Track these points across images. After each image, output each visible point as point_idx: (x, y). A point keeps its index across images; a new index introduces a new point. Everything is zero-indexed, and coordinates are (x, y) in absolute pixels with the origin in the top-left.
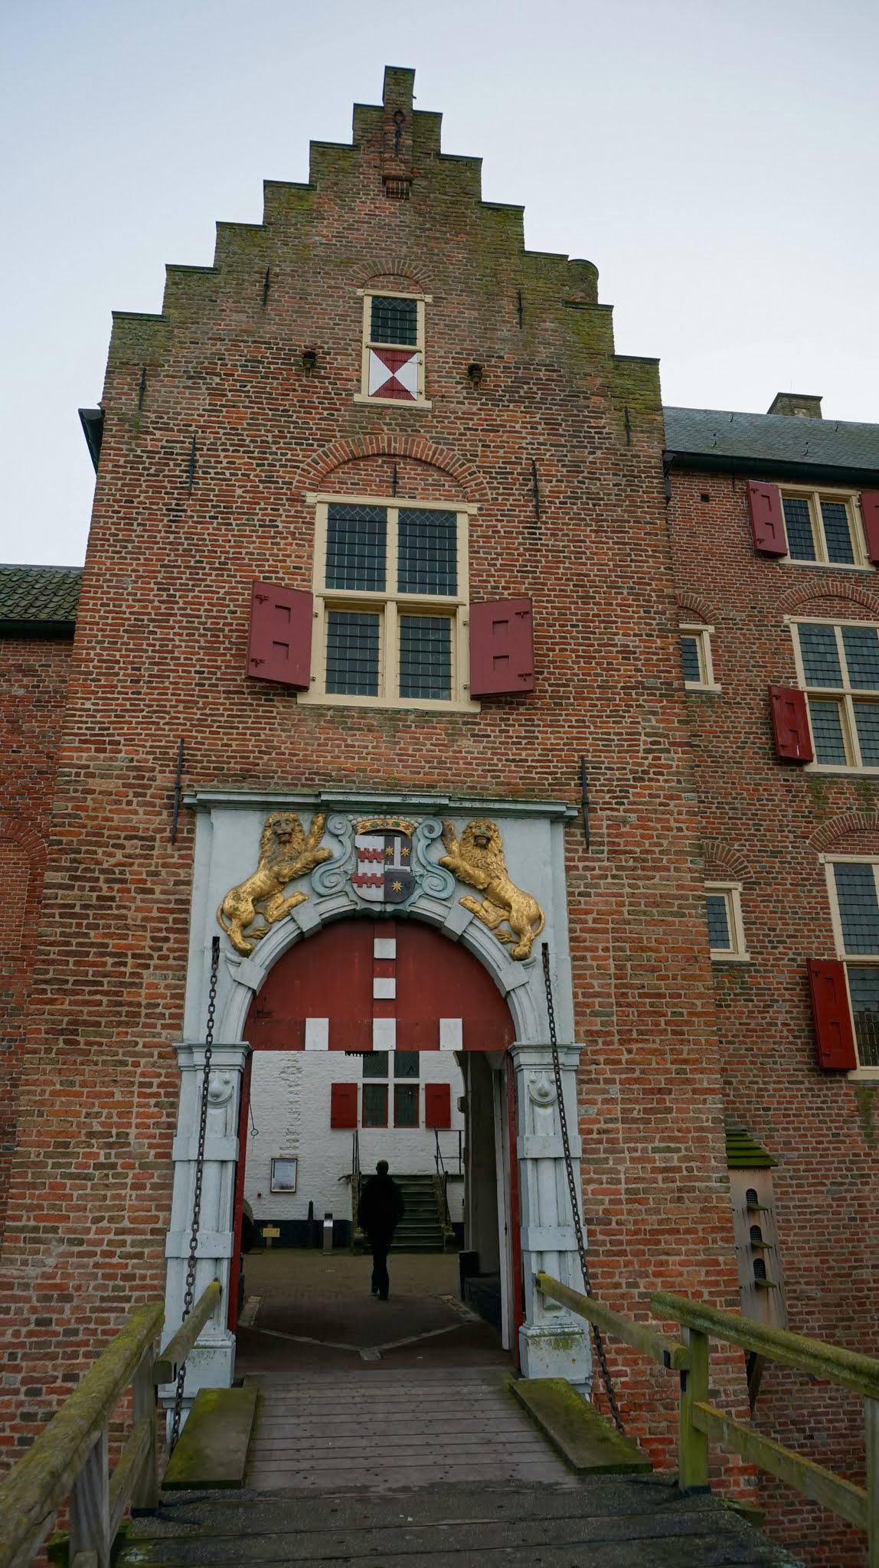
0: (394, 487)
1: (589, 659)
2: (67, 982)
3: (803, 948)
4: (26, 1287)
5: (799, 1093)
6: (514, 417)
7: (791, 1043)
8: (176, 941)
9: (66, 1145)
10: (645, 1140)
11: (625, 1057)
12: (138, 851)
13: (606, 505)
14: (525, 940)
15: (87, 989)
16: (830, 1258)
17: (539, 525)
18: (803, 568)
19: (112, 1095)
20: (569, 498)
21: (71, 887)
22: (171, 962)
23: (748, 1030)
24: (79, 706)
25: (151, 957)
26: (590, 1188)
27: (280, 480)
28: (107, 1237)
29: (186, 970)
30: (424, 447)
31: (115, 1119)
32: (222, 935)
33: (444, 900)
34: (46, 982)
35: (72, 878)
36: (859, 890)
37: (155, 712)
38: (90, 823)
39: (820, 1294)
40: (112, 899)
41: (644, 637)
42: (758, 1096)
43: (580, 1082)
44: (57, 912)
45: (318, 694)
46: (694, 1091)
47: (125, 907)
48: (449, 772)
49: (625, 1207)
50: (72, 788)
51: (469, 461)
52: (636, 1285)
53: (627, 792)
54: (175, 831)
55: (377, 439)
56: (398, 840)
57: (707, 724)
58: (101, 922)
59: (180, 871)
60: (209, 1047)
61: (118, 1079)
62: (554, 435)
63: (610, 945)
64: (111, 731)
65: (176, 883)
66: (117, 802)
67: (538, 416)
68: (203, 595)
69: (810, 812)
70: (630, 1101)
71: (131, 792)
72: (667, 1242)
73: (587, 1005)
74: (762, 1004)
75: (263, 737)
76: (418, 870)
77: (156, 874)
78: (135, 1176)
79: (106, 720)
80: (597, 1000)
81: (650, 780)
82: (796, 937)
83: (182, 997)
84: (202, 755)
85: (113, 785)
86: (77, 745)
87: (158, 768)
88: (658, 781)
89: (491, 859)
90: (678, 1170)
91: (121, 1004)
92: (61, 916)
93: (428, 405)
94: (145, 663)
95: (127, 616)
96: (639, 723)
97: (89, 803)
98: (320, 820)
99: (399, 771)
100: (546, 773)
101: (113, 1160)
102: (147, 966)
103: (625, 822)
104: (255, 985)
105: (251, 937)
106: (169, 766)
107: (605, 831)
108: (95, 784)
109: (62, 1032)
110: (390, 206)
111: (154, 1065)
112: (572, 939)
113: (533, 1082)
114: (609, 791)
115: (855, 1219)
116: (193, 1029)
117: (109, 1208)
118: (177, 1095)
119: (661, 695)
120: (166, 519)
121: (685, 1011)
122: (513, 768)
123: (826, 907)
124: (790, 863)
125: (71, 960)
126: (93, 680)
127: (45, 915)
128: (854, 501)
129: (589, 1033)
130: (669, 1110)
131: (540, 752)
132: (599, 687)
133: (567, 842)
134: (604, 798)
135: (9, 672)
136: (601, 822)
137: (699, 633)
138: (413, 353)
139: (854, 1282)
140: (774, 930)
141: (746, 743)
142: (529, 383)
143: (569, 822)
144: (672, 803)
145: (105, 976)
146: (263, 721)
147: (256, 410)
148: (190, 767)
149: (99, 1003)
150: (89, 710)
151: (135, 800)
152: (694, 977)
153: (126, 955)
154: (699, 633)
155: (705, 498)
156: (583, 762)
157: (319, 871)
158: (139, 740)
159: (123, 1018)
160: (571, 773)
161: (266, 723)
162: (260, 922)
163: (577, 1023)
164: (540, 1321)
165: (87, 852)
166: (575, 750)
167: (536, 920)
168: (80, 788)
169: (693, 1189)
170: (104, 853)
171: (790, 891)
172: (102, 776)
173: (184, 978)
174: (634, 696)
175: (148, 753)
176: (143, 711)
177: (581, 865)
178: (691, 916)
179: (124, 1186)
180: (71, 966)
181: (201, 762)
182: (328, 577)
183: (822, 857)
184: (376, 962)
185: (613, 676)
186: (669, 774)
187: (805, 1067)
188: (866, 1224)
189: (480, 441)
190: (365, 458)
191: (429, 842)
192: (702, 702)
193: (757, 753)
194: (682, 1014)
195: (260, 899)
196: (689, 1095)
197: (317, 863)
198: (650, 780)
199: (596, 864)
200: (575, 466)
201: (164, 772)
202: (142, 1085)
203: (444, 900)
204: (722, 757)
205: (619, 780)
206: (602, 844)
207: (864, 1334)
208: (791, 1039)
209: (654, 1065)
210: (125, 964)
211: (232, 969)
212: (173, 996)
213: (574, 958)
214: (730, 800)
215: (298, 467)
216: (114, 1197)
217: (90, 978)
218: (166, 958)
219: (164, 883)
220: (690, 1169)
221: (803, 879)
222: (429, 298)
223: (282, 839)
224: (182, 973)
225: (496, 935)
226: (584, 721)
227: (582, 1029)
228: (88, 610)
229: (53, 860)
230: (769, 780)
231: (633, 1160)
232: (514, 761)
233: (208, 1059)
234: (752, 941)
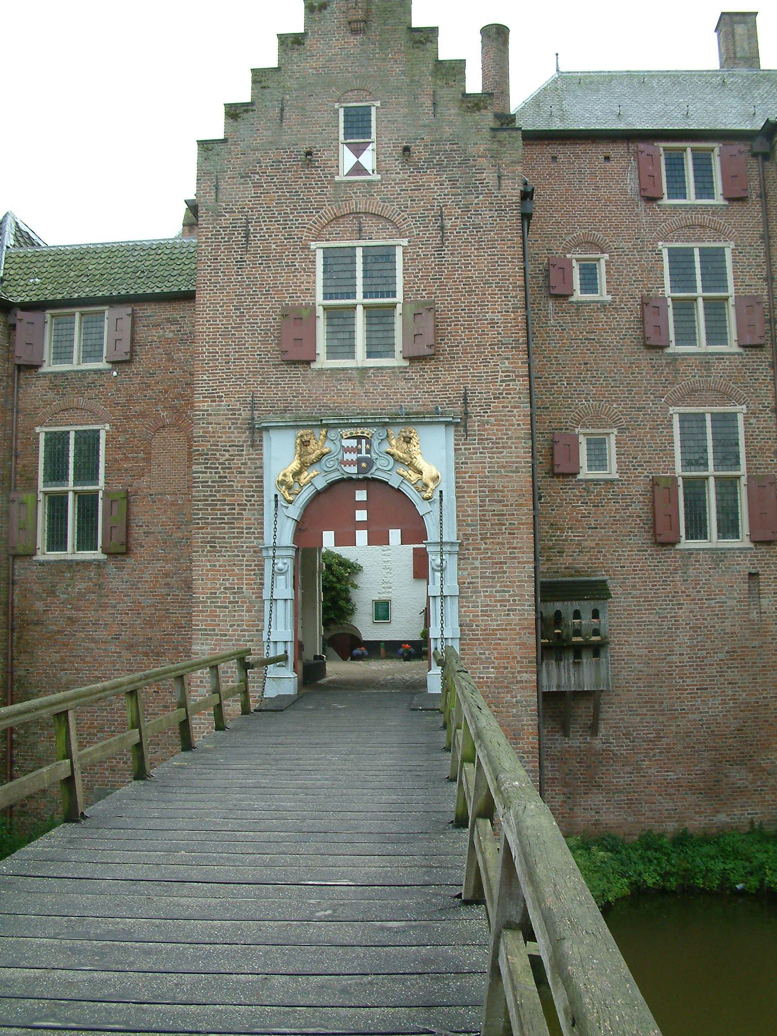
0: (360, 233)
3: (654, 469)
5: (644, 557)
6: (430, 178)
7: (642, 528)
9: (215, 593)
10: (492, 587)
13: (484, 231)
14: (429, 490)
16: (654, 650)
17: (444, 248)
18: (675, 206)
19: (234, 570)
20: (462, 229)
23: (614, 520)
25: (246, 505)
26: (463, 610)
27: (295, 237)
31: (236, 581)
32: (278, 493)
34: (199, 519)
35: (206, 468)
36: (695, 431)
38: (212, 440)
39: (646, 669)
40: (226, 477)
41: (504, 313)
42: (617, 559)
43: (460, 559)
44: (200, 485)
45: (323, 362)
46: (519, 563)
49: (480, 618)
51: (403, 211)
52: (484, 654)
54: (253, 441)
55: (349, 204)
56: (364, 441)
57: (600, 324)
60: (275, 548)
62: (454, 188)
63: (478, 489)
67: (445, 176)
68: (258, 310)
69: (666, 380)
70: (485, 568)
73: (464, 521)
74: (625, 504)
75: (294, 388)
76: (374, 456)
77: (245, 464)
80: (469, 519)
81: (503, 398)
82: (650, 462)
83: (262, 523)
85: (220, 419)
88: (508, 398)
90: (509, 601)
91: (234, 528)
93: (379, 177)
94: (231, 352)
95: (220, 326)
96: (498, 365)
97: (210, 429)
98: (324, 432)
101: (237, 599)
102: (245, 510)
103: (488, 423)
107: (476, 428)
109: (208, 542)
111: (251, 556)
113: (433, 560)
114: (479, 406)
115: (671, 629)
116: (268, 540)
117: (237, 621)
118: (263, 570)
119: (512, 348)
120: (235, 267)
121: (516, 523)
124: (650, 415)
125: (209, 508)
126: (206, 364)
127: (195, 487)
128: (717, 151)
129: (465, 535)
130: (505, 572)
132: (476, 345)
133: (456, 435)
135: (162, 322)
136: (474, 425)
137: (598, 260)
138: (369, 143)
139: (668, 663)
140: (636, 458)
141: (626, 335)
142: (439, 155)
143: (457, 424)
144: (515, 410)
145: (225, 515)
147: (280, 194)
149: (224, 528)
151: (232, 426)
152: (521, 505)
153: (234, 505)
154: (598, 260)
155: (607, 158)
156: (466, 390)
157: (325, 458)
159: (236, 535)
160: (459, 397)
162: (297, 488)
163: (459, 530)
165: (211, 454)
166: (461, 384)
171: (648, 433)
172: (215, 415)
173: (263, 514)
174: (496, 349)
177: (463, 447)
178: (522, 472)
179: (243, 611)
180: (209, 511)
185: (484, 338)
186: (514, 394)
187: (649, 541)
188: (678, 631)
189: (410, 197)
192: (598, 309)
193: (632, 342)
194: (514, 524)
195: (297, 474)
196: (516, 565)
197: (323, 455)
198: (503, 398)
199: (471, 446)
200: (466, 208)
202: (247, 566)
204: (609, 346)
205: (485, 399)
207: (670, 690)
208: (642, 525)
209: (498, 550)
210: (234, 509)
211: (284, 510)
214: (613, 375)
215: (305, 227)
218: (254, 505)
219: (250, 468)
220: (514, 601)
221: (657, 425)
222: (378, 104)
223: (305, 444)
225: (415, 488)
226: (467, 367)
228: (200, 325)
229: (196, 460)
230: (640, 360)
232: (427, 392)
233: (274, 553)
234: (621, 466)
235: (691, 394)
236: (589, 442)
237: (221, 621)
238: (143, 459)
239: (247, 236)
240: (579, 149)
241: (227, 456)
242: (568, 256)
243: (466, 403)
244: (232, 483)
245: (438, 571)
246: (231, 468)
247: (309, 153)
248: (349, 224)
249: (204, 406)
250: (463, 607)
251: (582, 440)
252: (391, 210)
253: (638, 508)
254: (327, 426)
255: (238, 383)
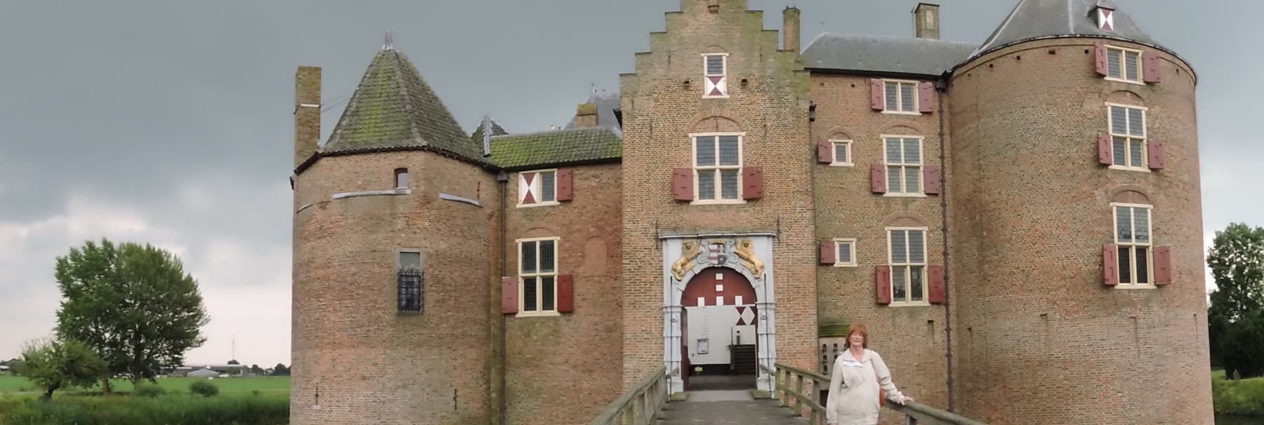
0: (717, 129)
1: (781, 183)
4: (630, 369)
11: (788, 305)
30: (727, 113)
43: (776, 313)
45: (697, 201)
46: (809, 314)
54: (657, 246)
60: (671, 307)
72: (798, 356)
83: (663, 293)
89: (749, 250)
93: (728, 97)
99: (723, 225)
103: (791, 235)
104: (683, 290)
108: (633, 233)
110: (712, 16)
116: (667, 302)
123: (886, 247)
129: (778, 299)
136: (783, 236)
138: (721, 77)
143: (774, 237)
152: (810, 282)
162: (683, 271)
164: (763, 376)
167: (762, 267)
169: (806, 342)
182: (698, 162)
183: (886, 228)
190: (707, 119)
196: (807, 316)
197: (699, 254)
213: (775, 277)
222: (727, 54)
223: (688, 248)
235: (897, 219)
236: (840, 245)
238: (581, 256)
239: (651, 129)
240: (837, 80)
242: (830, 140)
243: (778, 224)
247: (687, 82)
248: (712, 122)
249: (629, 226)
251: (837, 244)
252: (734, 115)
253: (868, 285)
254: (701, 238)
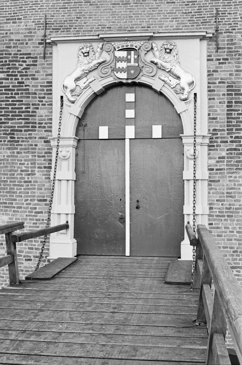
2: (9, 115)
8: (48, 98)
12: (31, 63)
14: (186, 92)
15: (17, 118)
21: (8, 79)
22: (47, 106)
24: (5, 5)
25: (39, 105)
26: (211, 191)
28: (30, 206)
29: (52, 109)
31: (30, 165)
33: (152, 77)
37: (34, 4)
40: (23, 83)
47: (28, 86)
48: (157, 20)
50: (5, 39)
53: (238, 24)
54: (45, 54)
58: (20, 92)
59: (48, 70)
60: (59, 138)
61: (30, 151)
64: (18, 14)
65: (47, 75)
66: (22, 44)
71: (27, 39)
76: (141, 65)
78: (38, 185)
79: (15, 10)
84: (54, 21)
85: (21, 37)
86: (5, 21)
87: (37, 28)
91: (29, 123)
92: (5, 90)
97: (12, 45)
98: (100, 46)
100: (200, 18)
101: (30, 180)
102: (38, 108)
105: (75, 95)
106: (41, 27)
109: (9, 134)
112: (209, 91)
114: (229, 24)
117: (29, 196)
122: (185, 16)
131: (197, 8)
134: (226, 27)
145: (23, 112)
146: (78, 4)
148: (49, 26)
150: (9, 6)
156: (218, 11)
158: (29, 17)
159: (30, 128)
161: (79, 5)
166: (214, 6)
168: (8, 39)
170: (19, 64)
173: (52, 112)
175: (33, 22)
176: (29, 4)
179: (34, 189)
181: (54, 24)
184: (127, 104)
191: (146, 52)
201: (39, 30)
203: (152, 77)
206: (224, 48)
210: (29, 108)
211: (68, 108)
212: (48, 119)
216: (31, 192)
217: (17, 114)
218: (45, 105)
224: (51, 110)
227: (212, 129)
231: (230, 181)
232: (186, 13)
237: (17, 196)
241: (25, 66)
244: (27, 87)
245: (191, 159)
246: (27, 75)
250: (211, 189)
255: (34, 8)
